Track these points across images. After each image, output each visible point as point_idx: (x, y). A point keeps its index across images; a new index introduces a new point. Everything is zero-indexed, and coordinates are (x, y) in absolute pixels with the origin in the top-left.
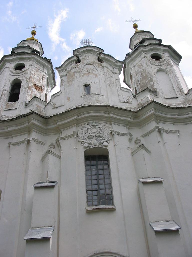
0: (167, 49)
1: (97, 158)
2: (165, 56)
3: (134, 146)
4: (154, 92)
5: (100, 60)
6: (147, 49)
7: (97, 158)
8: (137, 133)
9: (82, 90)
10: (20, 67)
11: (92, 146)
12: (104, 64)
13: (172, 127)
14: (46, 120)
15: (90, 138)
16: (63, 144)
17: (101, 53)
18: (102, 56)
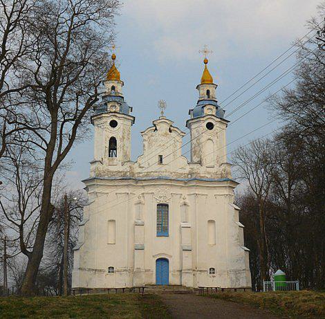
0: (219, 120)
1: (163, 207)
2: (217, 126)
3: (182, 201)
4: (200, 163)
5: (170, 131)
6: (204, 119)
7: (163, 207)
8: (185, 192)
9: (157, 159)
10: (113, 124)
11: (161, 202)
12: (173, 134)
13: (205, 192)
14: (137, 181)
15: (160, 197)
16: (146, 196)
17: (171, 126)
18: (172, 128)
